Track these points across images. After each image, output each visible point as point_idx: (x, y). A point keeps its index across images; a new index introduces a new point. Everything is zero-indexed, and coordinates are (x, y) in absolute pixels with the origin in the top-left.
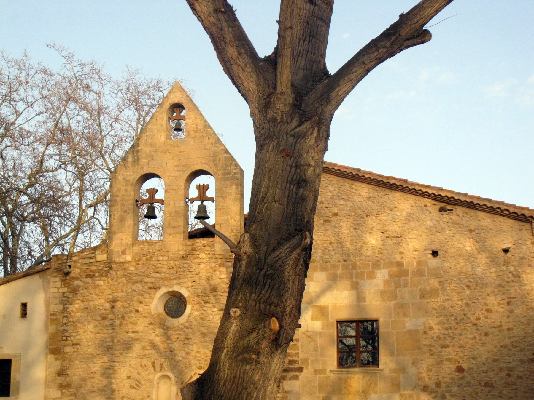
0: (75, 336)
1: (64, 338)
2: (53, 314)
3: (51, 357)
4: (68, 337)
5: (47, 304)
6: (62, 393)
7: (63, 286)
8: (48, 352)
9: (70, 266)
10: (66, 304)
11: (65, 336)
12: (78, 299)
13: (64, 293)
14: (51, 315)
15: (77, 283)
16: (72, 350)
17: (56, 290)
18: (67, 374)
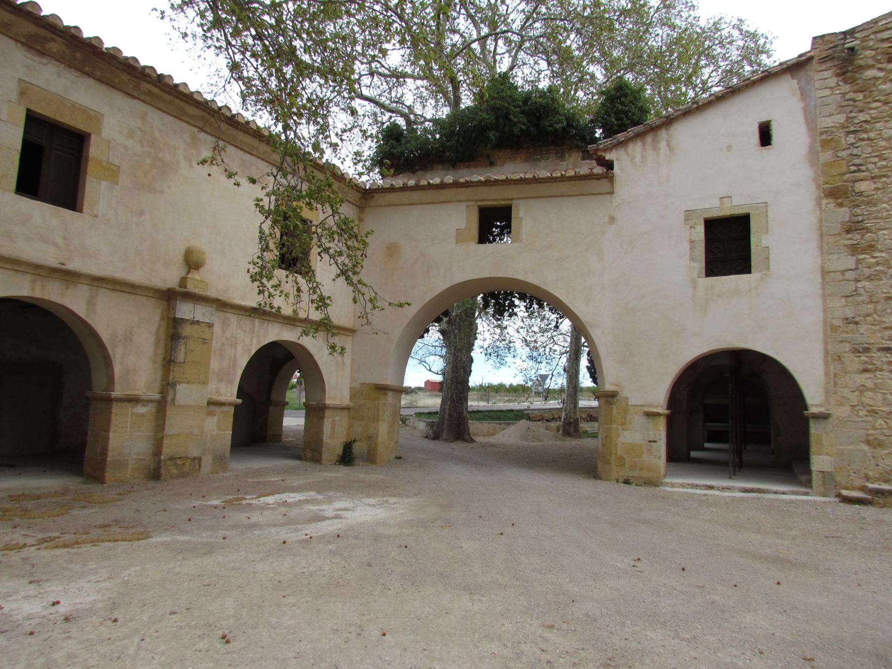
0: (875, 163)
1: (853, 168)
2: (826, 132)
3: (829, 204)
4: (861, 165)
5: (810, 117)
6: (858, 262)
7: (841, 83)
8: (822, 195)
9: (852, 49)
10: (851, 112)
11: (854, 165)
12: (878, 101)
13: (844, 94)
14: (821, 134)
15: (870, 73)
16: (873, 186)
17: (828, 92)
18: (867, 228)
